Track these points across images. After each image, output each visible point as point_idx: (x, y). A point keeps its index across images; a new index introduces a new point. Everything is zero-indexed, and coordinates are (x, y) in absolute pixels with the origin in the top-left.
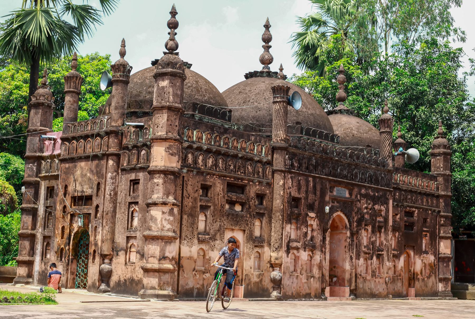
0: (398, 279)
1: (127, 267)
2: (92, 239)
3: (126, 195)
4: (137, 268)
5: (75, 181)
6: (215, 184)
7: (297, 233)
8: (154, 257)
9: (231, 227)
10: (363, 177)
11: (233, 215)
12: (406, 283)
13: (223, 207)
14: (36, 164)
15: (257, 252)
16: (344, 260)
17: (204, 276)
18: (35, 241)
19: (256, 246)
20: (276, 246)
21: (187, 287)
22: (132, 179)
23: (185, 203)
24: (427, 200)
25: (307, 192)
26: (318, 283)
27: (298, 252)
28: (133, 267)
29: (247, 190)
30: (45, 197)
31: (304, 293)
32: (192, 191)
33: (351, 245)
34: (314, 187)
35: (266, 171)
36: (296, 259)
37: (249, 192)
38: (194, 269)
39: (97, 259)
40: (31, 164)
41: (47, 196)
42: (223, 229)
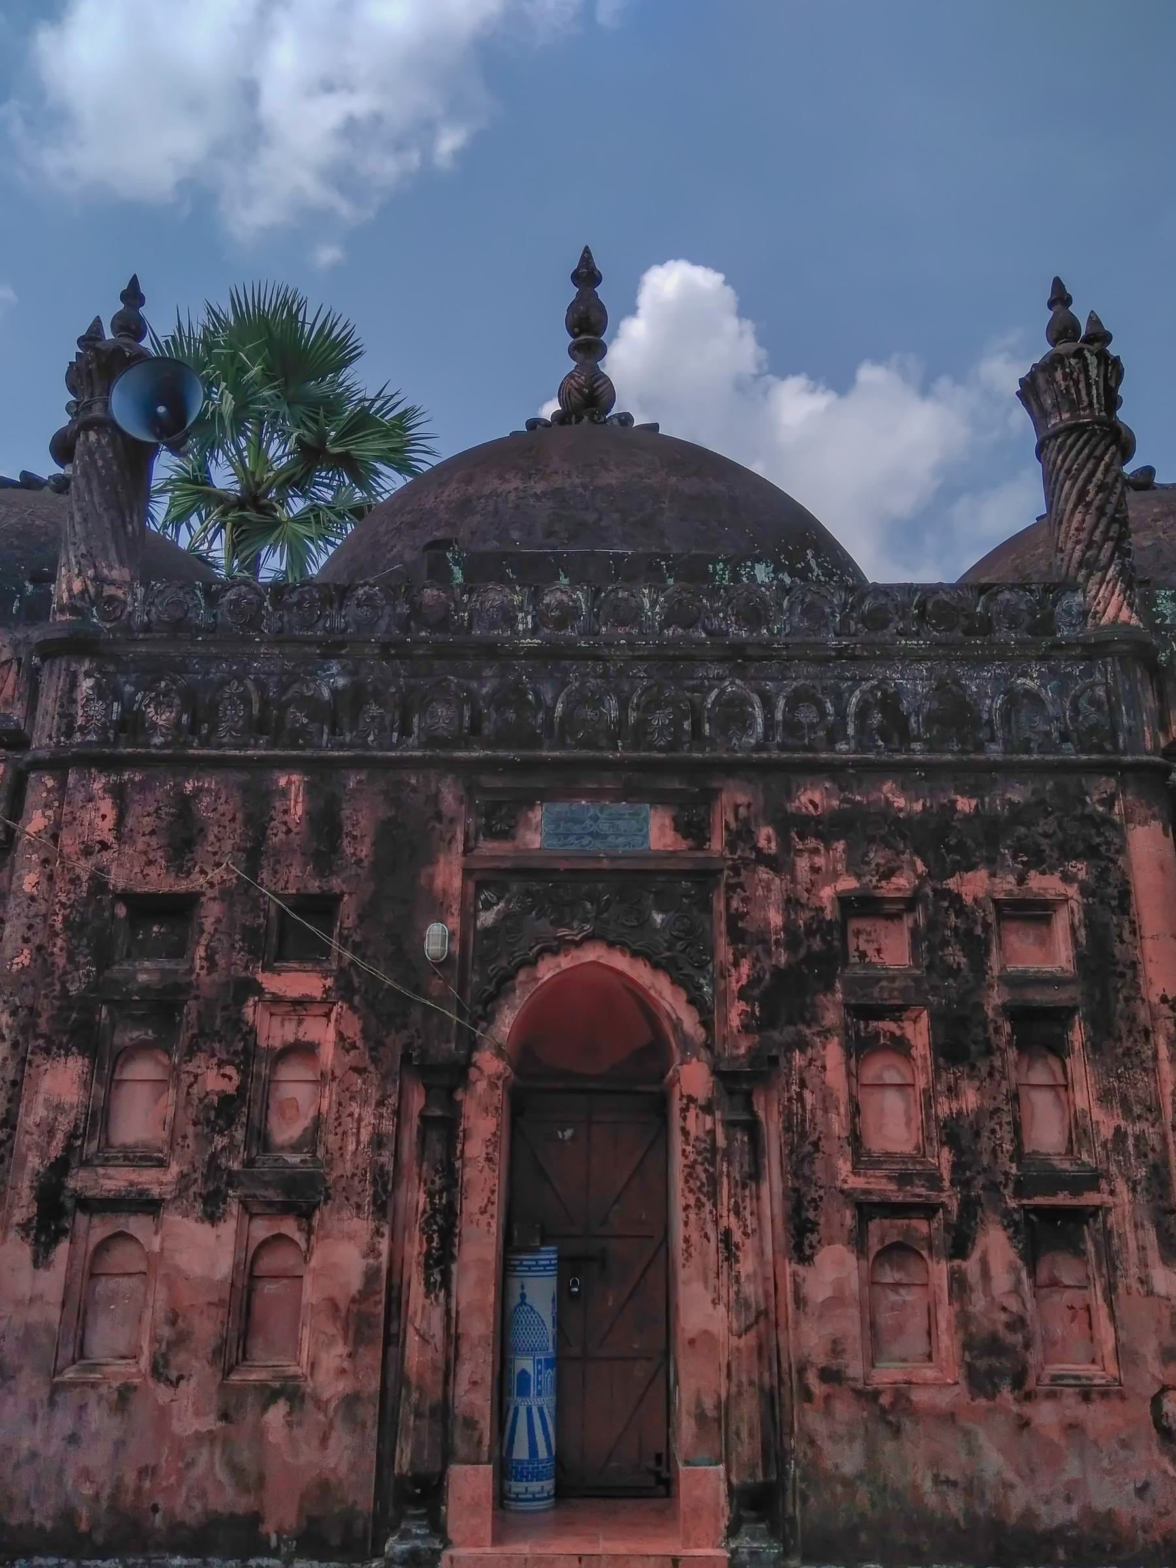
10: (807, 715)
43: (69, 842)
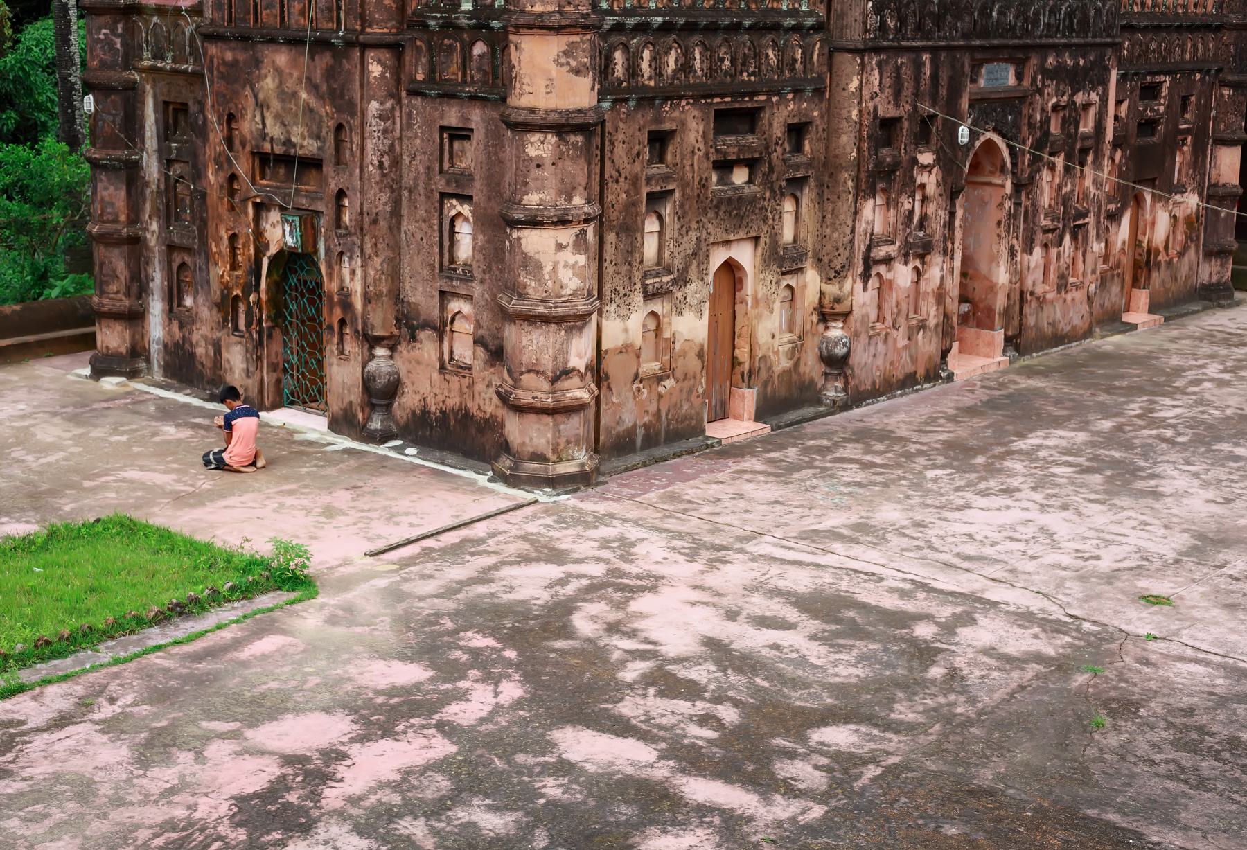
0: (1113, 276)
1: (447, 377)
2: (332, 286)
3: (428, 168)
4: (480, 387)
5: (262, 106)
6: (683, 123)
7: (886, 217)
8: (537, 372)
9: (726, 237)
10: (1053, 21)
11: (730, 200)
12: (1128, 278)
13: (704, 184)
14: (120, 31)
15: (788, 286)
16: (994, 259)
17: (661, 389)
18: (141, 254)
19: (784, 274)
20: (838, 264)
21: (621, 428)
22: (445, 123)
23: (610, 198)
24: (1194, 46)
25: (916, 94)
26: (934, 340)
27: (889, 270)
28: (466, 382)
29: (765, 122)
30: (162, 131)
31: (901, 377)
32: (626, 159)
33: (1013, 216)
34: (935, 77)
35: (813, 52)
36: (885, 288)
37: (771, 125)
38: (636, 376)
39: (351, 347)
40: (104, 31)
41: (166, 128)
42: (704, 249)
43: (866, 93)
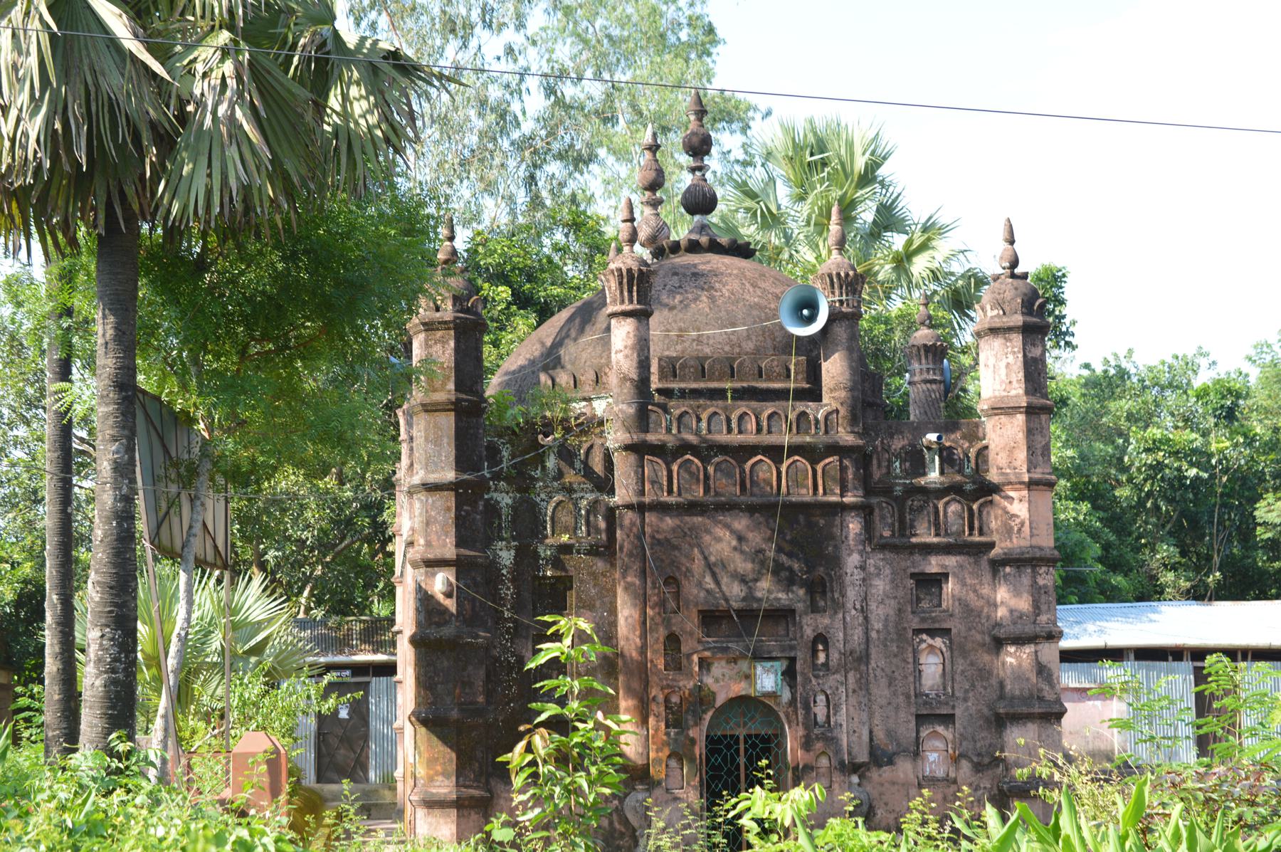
3: (899, 610)
14: (481, 508)
22: (916, 571)
40: (465, 508)
